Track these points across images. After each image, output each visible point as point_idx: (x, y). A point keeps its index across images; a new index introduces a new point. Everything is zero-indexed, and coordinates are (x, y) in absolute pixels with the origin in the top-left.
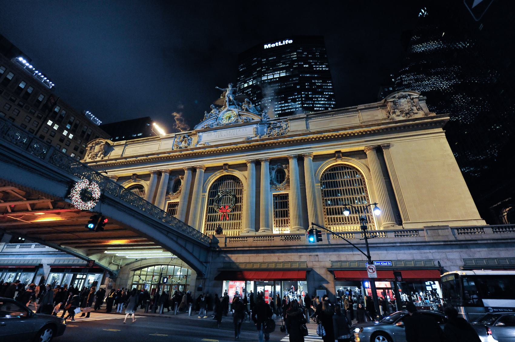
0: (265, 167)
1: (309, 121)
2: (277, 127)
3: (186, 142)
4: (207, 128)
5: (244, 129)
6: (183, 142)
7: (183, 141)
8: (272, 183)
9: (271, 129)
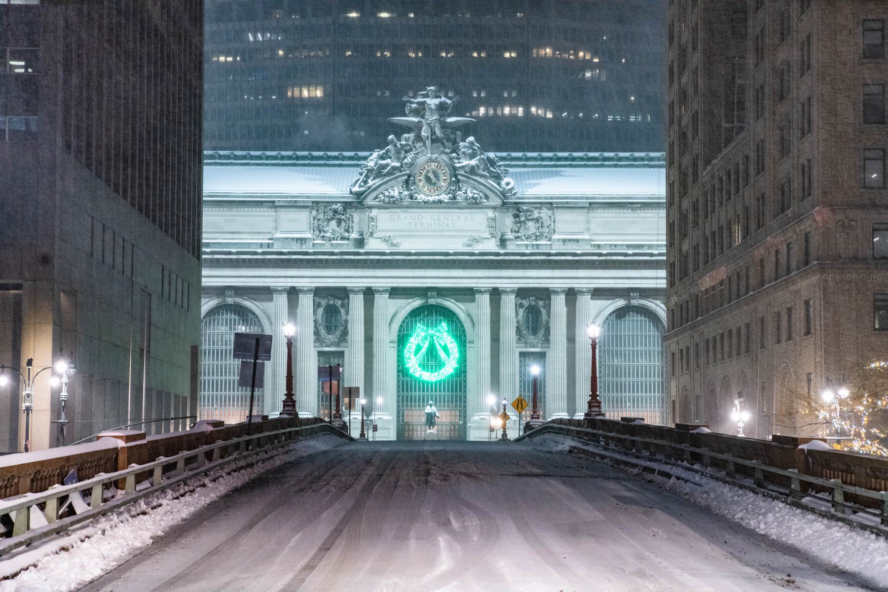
0: (509, 303)
1: (592, 215)
2: (533, 220)
3: (339, 222)
4: (389, 203)
5: (469, 216)
6: (333, 223)
7: (332, 219)
8: (519, 330)
9: (520, 222)
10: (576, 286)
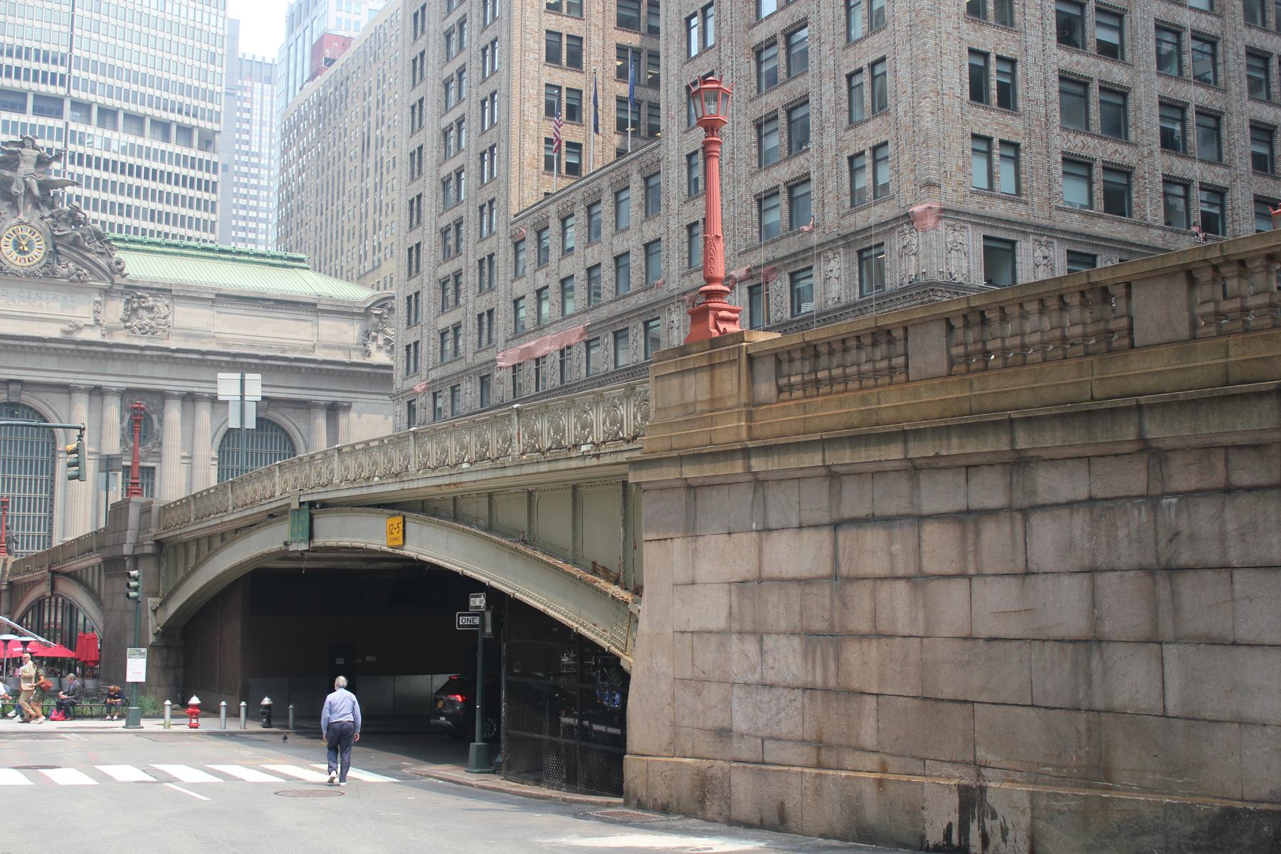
10: (196, 390)
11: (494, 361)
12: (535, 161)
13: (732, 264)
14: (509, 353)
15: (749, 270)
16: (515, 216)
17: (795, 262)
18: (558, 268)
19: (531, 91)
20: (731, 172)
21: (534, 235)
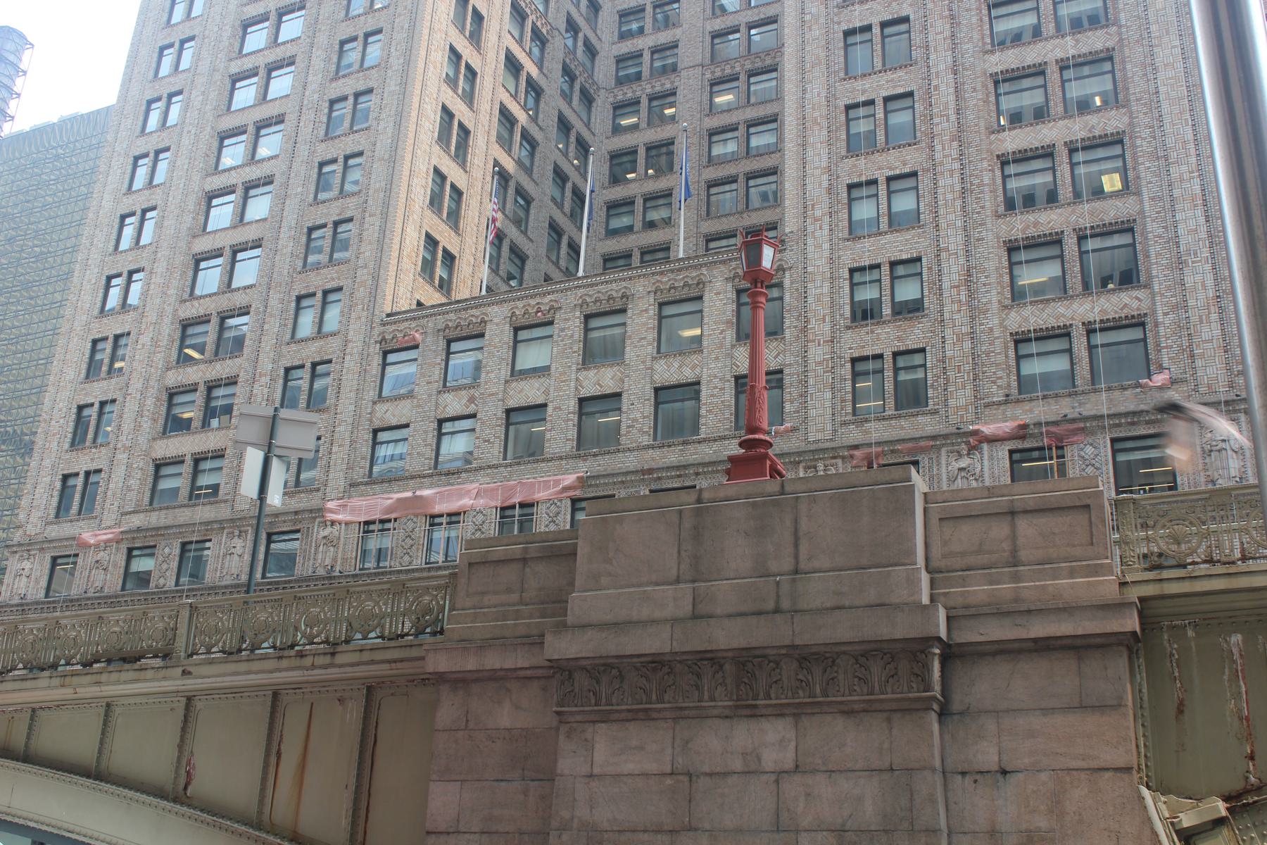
11: (320, 511)
12: (414, 255)
13: (970, 417)
14: (357, 502)
15: (1024, 427)
16: (388, 315)
17: (1133, 424)
18: (505, 391)
19: (421, 167)
20: (963, 298)
21: (442, 344)
